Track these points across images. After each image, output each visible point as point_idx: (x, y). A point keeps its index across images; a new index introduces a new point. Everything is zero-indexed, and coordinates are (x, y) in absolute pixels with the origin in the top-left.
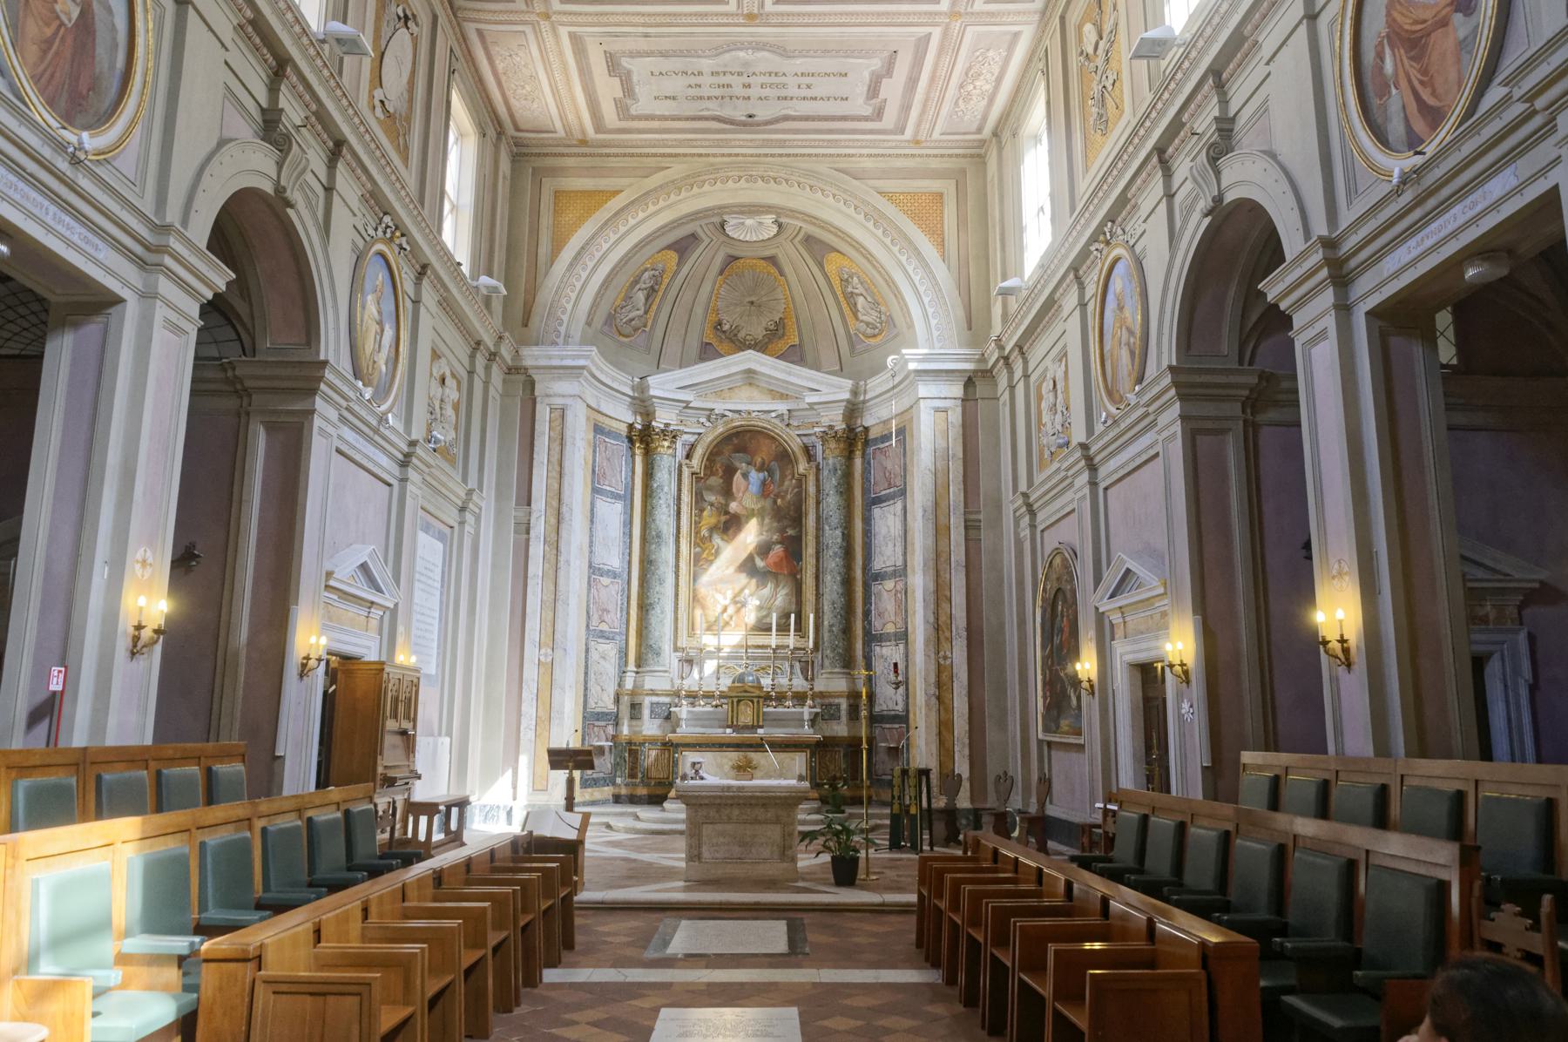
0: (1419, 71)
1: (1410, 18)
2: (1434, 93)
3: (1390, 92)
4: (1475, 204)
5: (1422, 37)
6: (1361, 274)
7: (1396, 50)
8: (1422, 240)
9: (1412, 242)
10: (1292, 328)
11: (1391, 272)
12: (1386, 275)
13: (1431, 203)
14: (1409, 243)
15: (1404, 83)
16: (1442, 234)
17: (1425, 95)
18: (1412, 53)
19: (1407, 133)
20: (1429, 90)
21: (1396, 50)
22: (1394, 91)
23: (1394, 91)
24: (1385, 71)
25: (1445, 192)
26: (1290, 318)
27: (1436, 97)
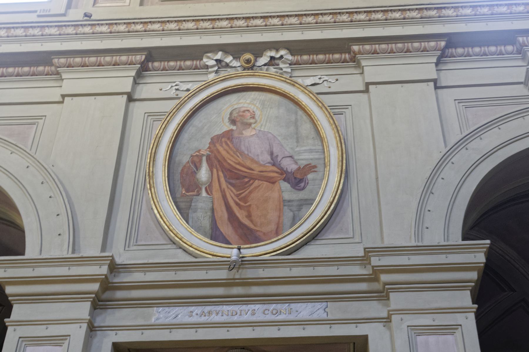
0: (237, 196)
1: (236, 159)
2: (249, 216)
3: (199, 194)
4: (278, 312)
5: (245, 177)
6: (120, 307)
7: (215, 171)
8: (210, 313)
9: (197, 310)
10: (9, 317)
11: (159, 322)
12: (153, 321)
13: (236, 290)
14: (192, 309)
15: (217, 195)
16: (236, 319)
17: (240, 215)
18: (233, 181)
19: (212, 229)
20: (245, 213)
21: (215, 171)
22: (204, 194)
23: (204, 194)
24: (198, 176)
25: (256, 290)
26: (10, 307)
27: (252, 221)
